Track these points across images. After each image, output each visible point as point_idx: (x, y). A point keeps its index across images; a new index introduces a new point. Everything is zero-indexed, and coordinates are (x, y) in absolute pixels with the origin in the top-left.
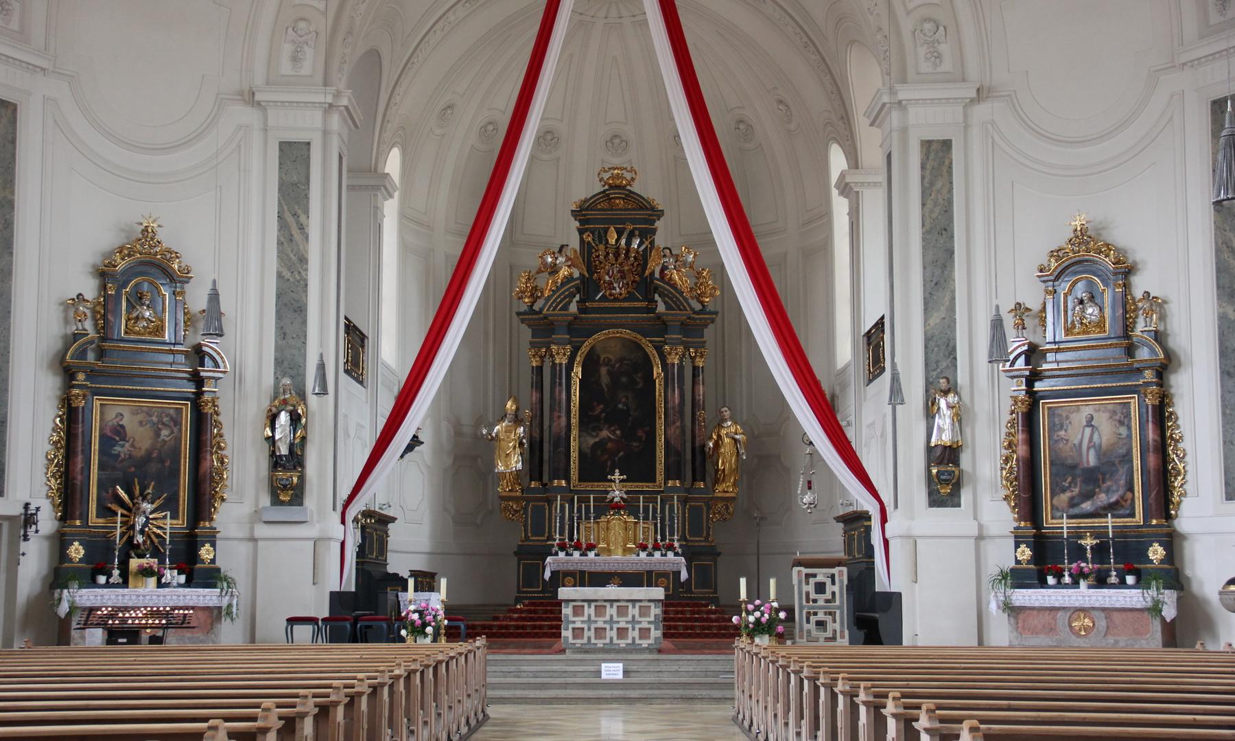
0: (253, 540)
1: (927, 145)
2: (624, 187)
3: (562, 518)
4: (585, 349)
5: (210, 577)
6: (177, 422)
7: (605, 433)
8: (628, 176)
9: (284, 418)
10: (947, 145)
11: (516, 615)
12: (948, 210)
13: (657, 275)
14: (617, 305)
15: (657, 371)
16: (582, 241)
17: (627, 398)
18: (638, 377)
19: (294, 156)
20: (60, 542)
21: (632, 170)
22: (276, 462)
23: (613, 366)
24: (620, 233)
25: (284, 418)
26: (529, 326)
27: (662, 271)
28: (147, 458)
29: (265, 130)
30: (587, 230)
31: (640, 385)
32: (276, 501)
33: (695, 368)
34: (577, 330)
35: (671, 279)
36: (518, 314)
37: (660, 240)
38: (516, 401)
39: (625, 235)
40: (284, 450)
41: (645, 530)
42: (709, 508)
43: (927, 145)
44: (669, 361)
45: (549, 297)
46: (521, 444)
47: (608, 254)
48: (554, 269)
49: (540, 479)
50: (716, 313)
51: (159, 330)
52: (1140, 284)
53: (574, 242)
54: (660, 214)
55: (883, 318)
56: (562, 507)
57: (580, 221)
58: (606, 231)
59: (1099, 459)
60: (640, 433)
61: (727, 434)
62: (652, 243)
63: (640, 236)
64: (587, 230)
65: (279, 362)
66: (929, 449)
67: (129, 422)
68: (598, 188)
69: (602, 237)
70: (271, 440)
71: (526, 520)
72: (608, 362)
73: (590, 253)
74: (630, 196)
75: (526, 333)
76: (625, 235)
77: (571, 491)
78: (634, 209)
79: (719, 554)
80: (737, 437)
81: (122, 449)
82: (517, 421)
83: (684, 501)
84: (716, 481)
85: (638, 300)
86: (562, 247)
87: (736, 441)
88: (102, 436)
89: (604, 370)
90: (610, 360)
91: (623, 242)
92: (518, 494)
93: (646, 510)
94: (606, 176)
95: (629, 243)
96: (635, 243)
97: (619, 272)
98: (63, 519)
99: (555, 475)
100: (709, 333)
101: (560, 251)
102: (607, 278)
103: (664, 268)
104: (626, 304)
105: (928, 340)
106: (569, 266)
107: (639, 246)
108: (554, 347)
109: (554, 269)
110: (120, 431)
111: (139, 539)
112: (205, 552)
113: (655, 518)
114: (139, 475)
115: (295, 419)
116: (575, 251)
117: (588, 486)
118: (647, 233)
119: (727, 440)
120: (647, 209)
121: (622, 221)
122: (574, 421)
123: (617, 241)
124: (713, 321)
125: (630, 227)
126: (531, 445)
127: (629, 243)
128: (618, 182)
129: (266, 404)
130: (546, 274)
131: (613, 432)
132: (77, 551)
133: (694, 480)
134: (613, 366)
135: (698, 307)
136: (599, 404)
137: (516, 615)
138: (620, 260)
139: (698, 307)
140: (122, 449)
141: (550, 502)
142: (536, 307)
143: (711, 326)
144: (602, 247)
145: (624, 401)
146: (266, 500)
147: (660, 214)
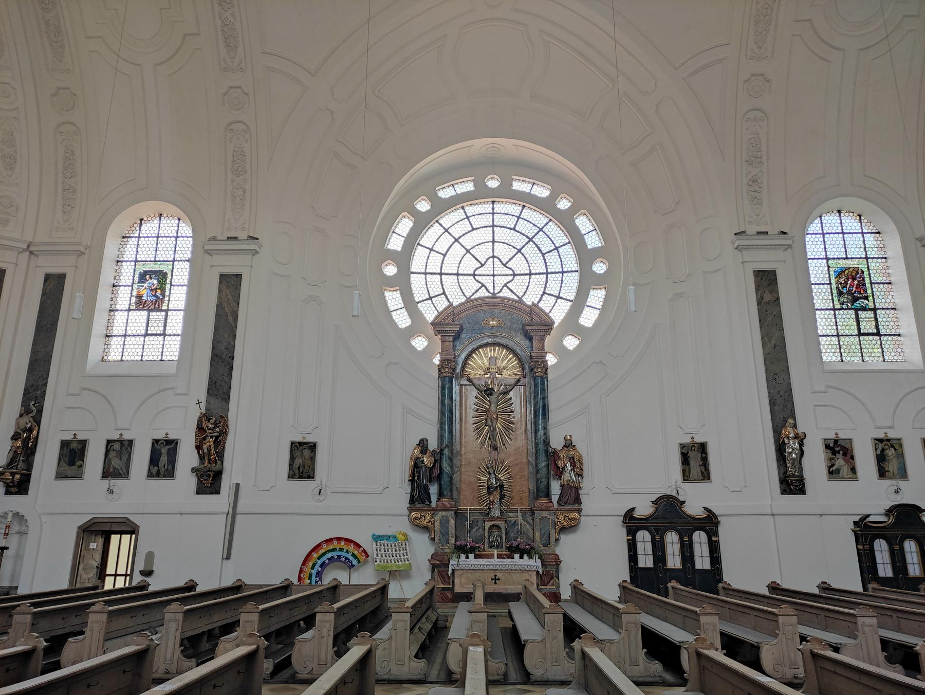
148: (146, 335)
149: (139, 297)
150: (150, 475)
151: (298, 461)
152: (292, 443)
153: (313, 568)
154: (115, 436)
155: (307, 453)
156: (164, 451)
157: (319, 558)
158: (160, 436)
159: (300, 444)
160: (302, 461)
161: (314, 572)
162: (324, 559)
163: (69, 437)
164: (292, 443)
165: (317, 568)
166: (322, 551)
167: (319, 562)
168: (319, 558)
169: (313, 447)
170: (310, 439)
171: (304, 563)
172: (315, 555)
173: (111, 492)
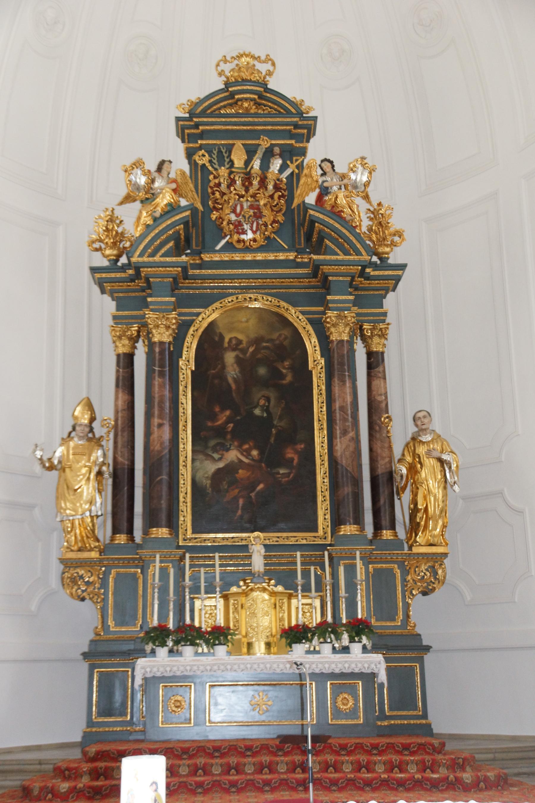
2: (257, 83)
3: (164, 590)
7: (233, 455)
8: (263, 68)
11: (64, 786)
14: (249, 257)
16: (193, 164)
17: (268, 399)
18: (284, 367)
21: (268, 59)
23: (244, 351)
24: (251, 152)
26: (112, 294)
27: (320, 199)
30: (200, 148)
31: (289, 378)
33: (370, 355)
34: (187, 294)
35: (335, 205)
36: (94, 270)
38: (89, 406)
39: (259, 154)
42: (405, 572)
44: (334, 337)
45: (143, 236)
46: (99, 473)
47: (232, 182)
48: (149, 196)
49: (130, 531)
50: (403, 267)
53: (181, 164)
56: (164, 572)
57: (192, 138)
58: (230, 149)
60: (290, 454)
61: (429, 453)
62: (300, 167)
63: (281, 156)
64: (200, 148)
68: (219, 84)
69: (223, 157)
71: (105, 600)
72: (236, 345)
73: (205, 182)
74: (265, 95)
75: (109, 305)
76: (259, 154)
77: (179, 547)
78: (270, 115)
79: (428, 648)
80: (445, 457)
82: (96, 442)
83: (367, 560)
84: (414, 528)
85: (283, 250)
86: (162, 164)
87: (441, 461)
89: (230, 357)
90: (240, 342)
91: (256, 164)
92: (94, 555)
93: (306, 574)
94: (227, 68)
95: (265, 166)
96: (276, 164)
97: (251, 207)
99: (152, 520)
100: (390, 301)
101: (159, 169)
102: (233, 217)
103: (324, 191)
104: (260, 257)
106: (175, 191)
107: (282, 169)
108: (150, 316)
109: (149, 196)
113: (319, 587)
116: (183, 173)
118: (293, 154)
119: (430, 463)
120: (288, 113)
121: (256, 135)
123: (247, 163)
124: (398, 279)
125: (265, 143)
126: (115, 475)
127: (265, 166)
128: (245, 75)
130: (137, 205)
131: (247, 453)
133: (378, 527)
134: (244, 351)
135: (375, 259)
136: (223, 409)
137: (64, 786)
138: (252, 191)
139: (375, 259)
141: (144, 565)
142: (123, 260)
143: (391, 295)
144: (223, 171)
145: (263, 404)
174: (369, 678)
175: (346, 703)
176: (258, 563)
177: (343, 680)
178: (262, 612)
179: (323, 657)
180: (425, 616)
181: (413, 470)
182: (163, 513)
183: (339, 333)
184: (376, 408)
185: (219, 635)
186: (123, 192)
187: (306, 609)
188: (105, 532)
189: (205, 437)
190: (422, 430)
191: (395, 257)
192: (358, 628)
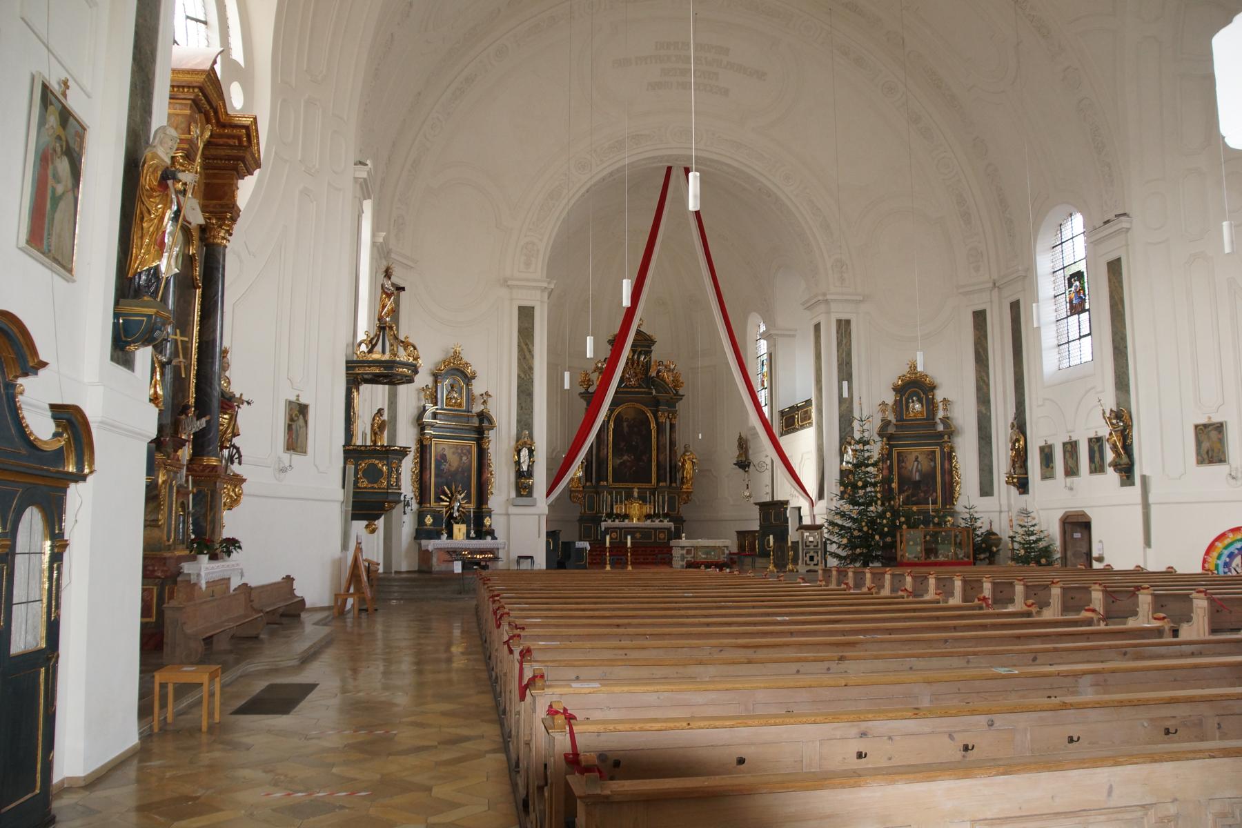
0: (508, 515)
1: (839, 322)
4: (616, 413)
5: (491, 533)
6: (470, 453)
7: (625, 458)
9: (525, 452)
10: (848, 322)
12: (849, 354)
13: (654, 374)
15: (653, 425)
19: (526, 314)
20: (421, 517)
22: (520, 474)
25: (525, 452)
28: (456, 472)
29: (512, 299)
32: (519, 494)
37: (655, 356)
40: (525, 468)
41: (648, 509)
43: (839, 322)
51: (460, 405)
52: (939, 395)
54: (654, 342)
55: (808, 402)
59: (921, 475)
65: (519, 421)
66: (841, 471)
67: (449, 454)
70: (518, 463)
72: (627, 420)
81: (445, 467)
84: (683, 483)
88: (436, 460)
95: (639, 358)
98: (421, 503)
100: (680, 406)
105: (841, 417)
110: (444, 457)
111: (456, 514)
112: (487, 521)
114: (451, 481)
115: (531, 452)
117: (617, 485)
118: (648, 353)
122: (610, 451)
129: (513, 443)
132: (429, 520)
140: (445, 467)
146: (513, 494)
147: (654, 342)
148: (1081, 337)
149: (1071, 301)
150: (1091, 472)
151: (1206, 445)
152: (1196, 427)
153: (1219, 557)
154: (1067, 440)
155: (1214, 434)
156: (1096, 448)
157: (1225, 548)
158: (1092, 435)
159: (1205, 426)
160: (1211, 443)
161: (1221, 563)
162: (1232, 549)
163: (1043, 444)
164: (1196, 427)
165: (1225, 558)
166: (1226, 542)
167: (1226, 552)
168: (1225, 548)
169: (1220, 427)
170: (1216, 419)
171: (1208, 552)
172: (1219, 545)
173: (1071, 489)
174: (669, 529)
175: (662, 536)
176: (636, 494)
177: (661, 530)
178: (635, 509)
179: (657, 523)
180: (685, 511)
181: (683, 464)
182: (601, 476)
183: (662, 420)
184: (672, 444)
185: (626, 516)
186: (593, 367)
187: (648, 509)
188: (583, 481)
189: (617, 451)
190: (686, 451)
191: (681, 392)
192: (666, 516)
